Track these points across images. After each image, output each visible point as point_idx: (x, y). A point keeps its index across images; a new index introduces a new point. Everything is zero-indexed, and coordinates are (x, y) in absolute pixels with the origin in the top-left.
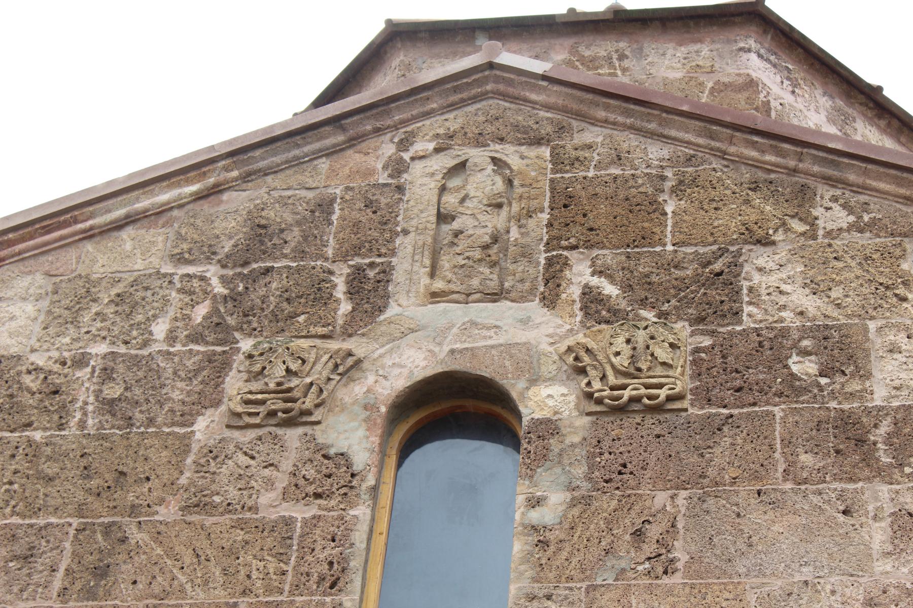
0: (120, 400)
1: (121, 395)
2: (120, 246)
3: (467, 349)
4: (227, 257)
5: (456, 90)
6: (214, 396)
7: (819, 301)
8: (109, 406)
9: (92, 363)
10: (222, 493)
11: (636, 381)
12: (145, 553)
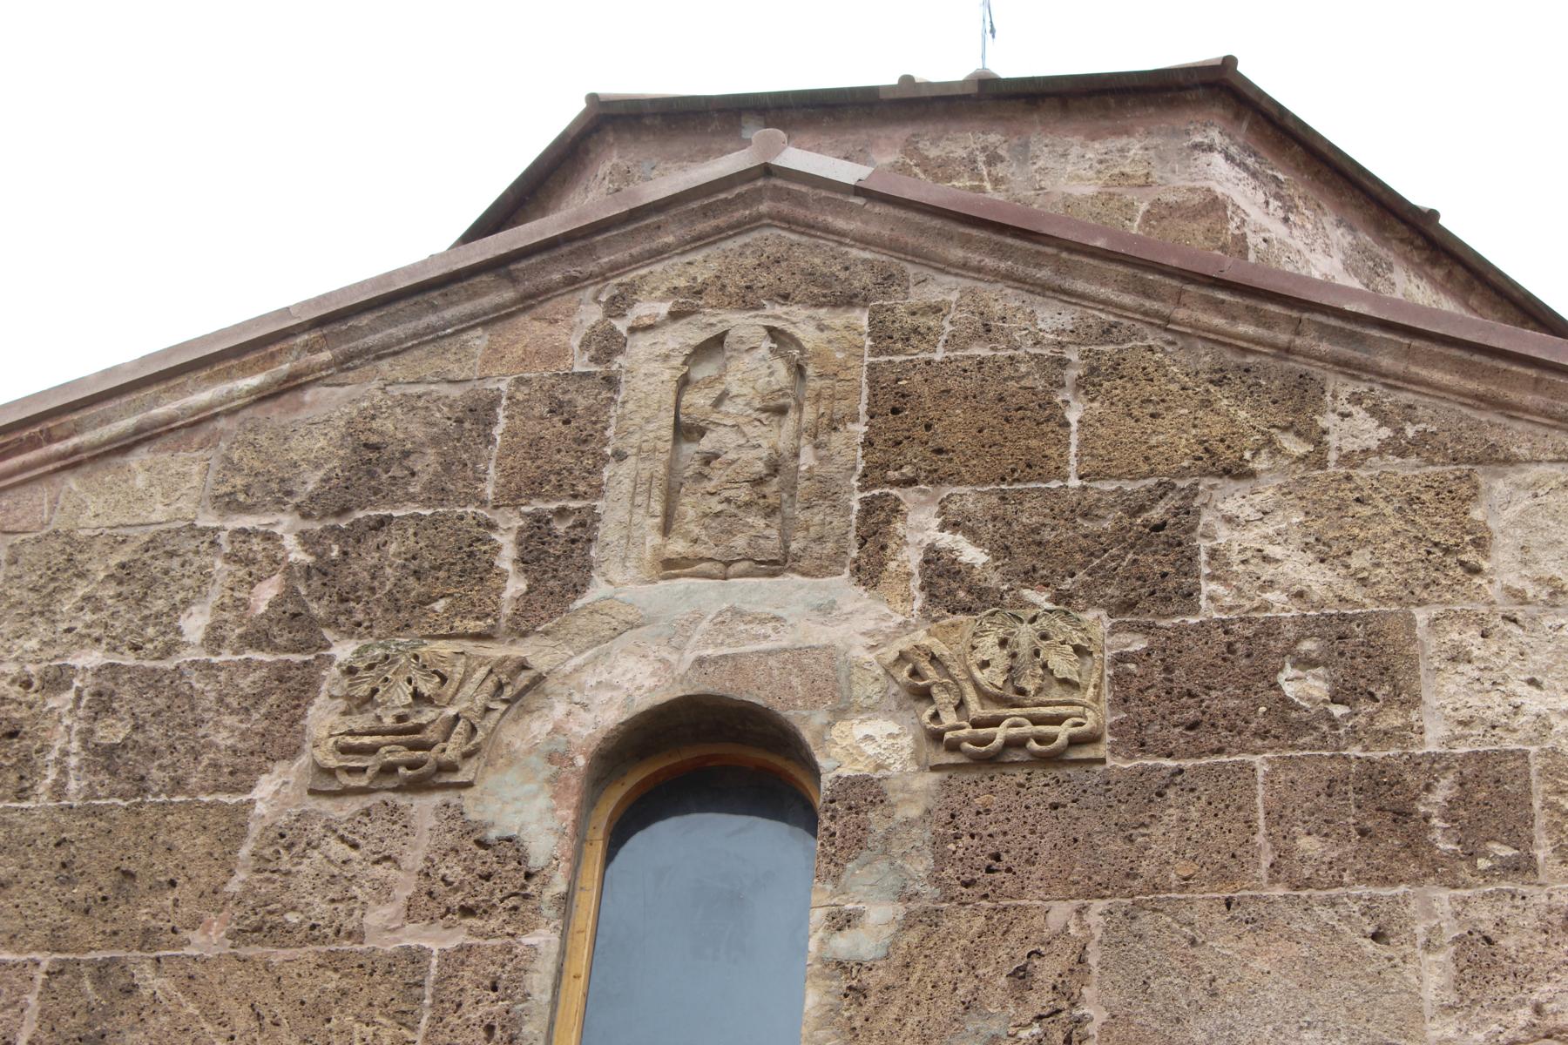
0: (125, 746)
1: (127, 738)
2: (126, 481)
3: (725, 657)
4: (311, 499)
5: (706, 212)
6: (288, 740)
7: (1330, 573)
8: (105, 757)
9: (77, 683)
10: (301, 907)
11: (1017, 711)
12: (167, 1012)
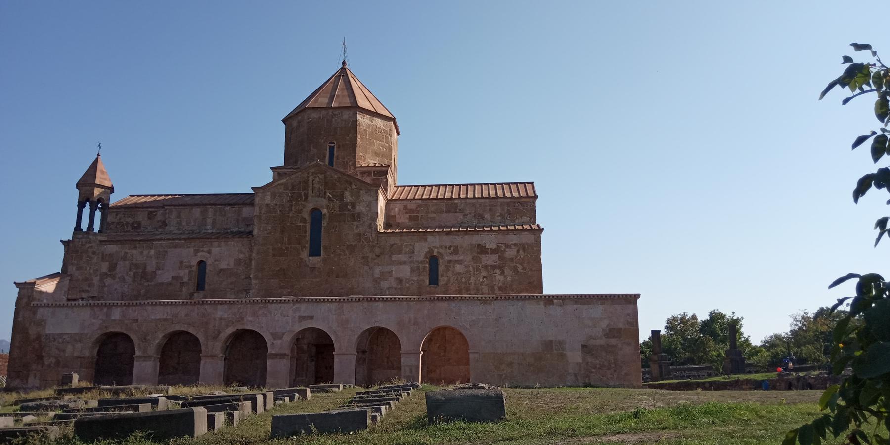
8: (280, 211)
